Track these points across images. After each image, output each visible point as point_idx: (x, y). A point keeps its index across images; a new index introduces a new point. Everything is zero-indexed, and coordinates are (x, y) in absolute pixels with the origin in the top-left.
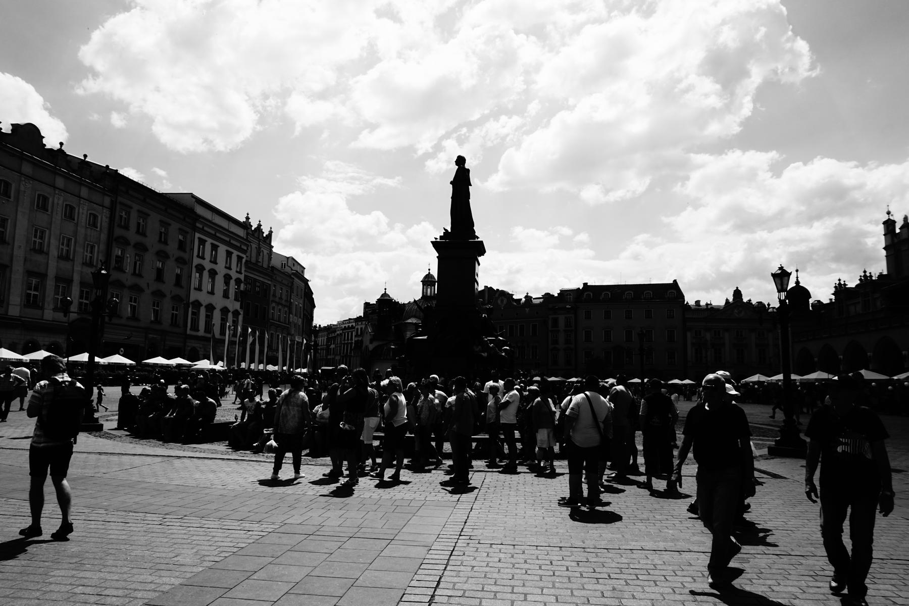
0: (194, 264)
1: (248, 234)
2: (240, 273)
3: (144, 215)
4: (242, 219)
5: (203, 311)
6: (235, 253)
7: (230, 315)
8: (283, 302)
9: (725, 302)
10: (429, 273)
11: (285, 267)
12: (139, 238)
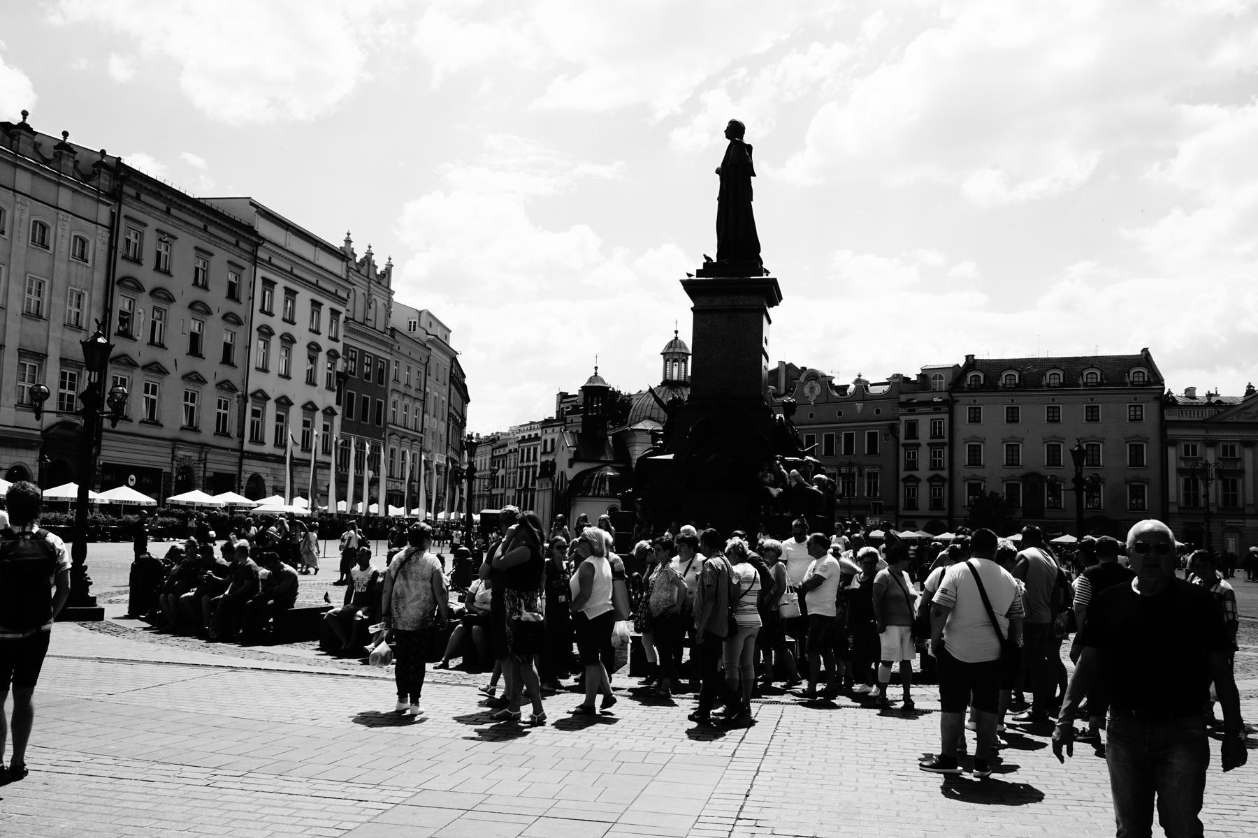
0: (255, 326)
1: (348, 269)
2: (336, 340)
3: (166, 238)
4: (338, 243)
5: (271, 410)
6: (327, 304)
7: (319, 416)
8: (412, 392)
9: (1245, 391)
10: (676, 338)
11: (414, 330)
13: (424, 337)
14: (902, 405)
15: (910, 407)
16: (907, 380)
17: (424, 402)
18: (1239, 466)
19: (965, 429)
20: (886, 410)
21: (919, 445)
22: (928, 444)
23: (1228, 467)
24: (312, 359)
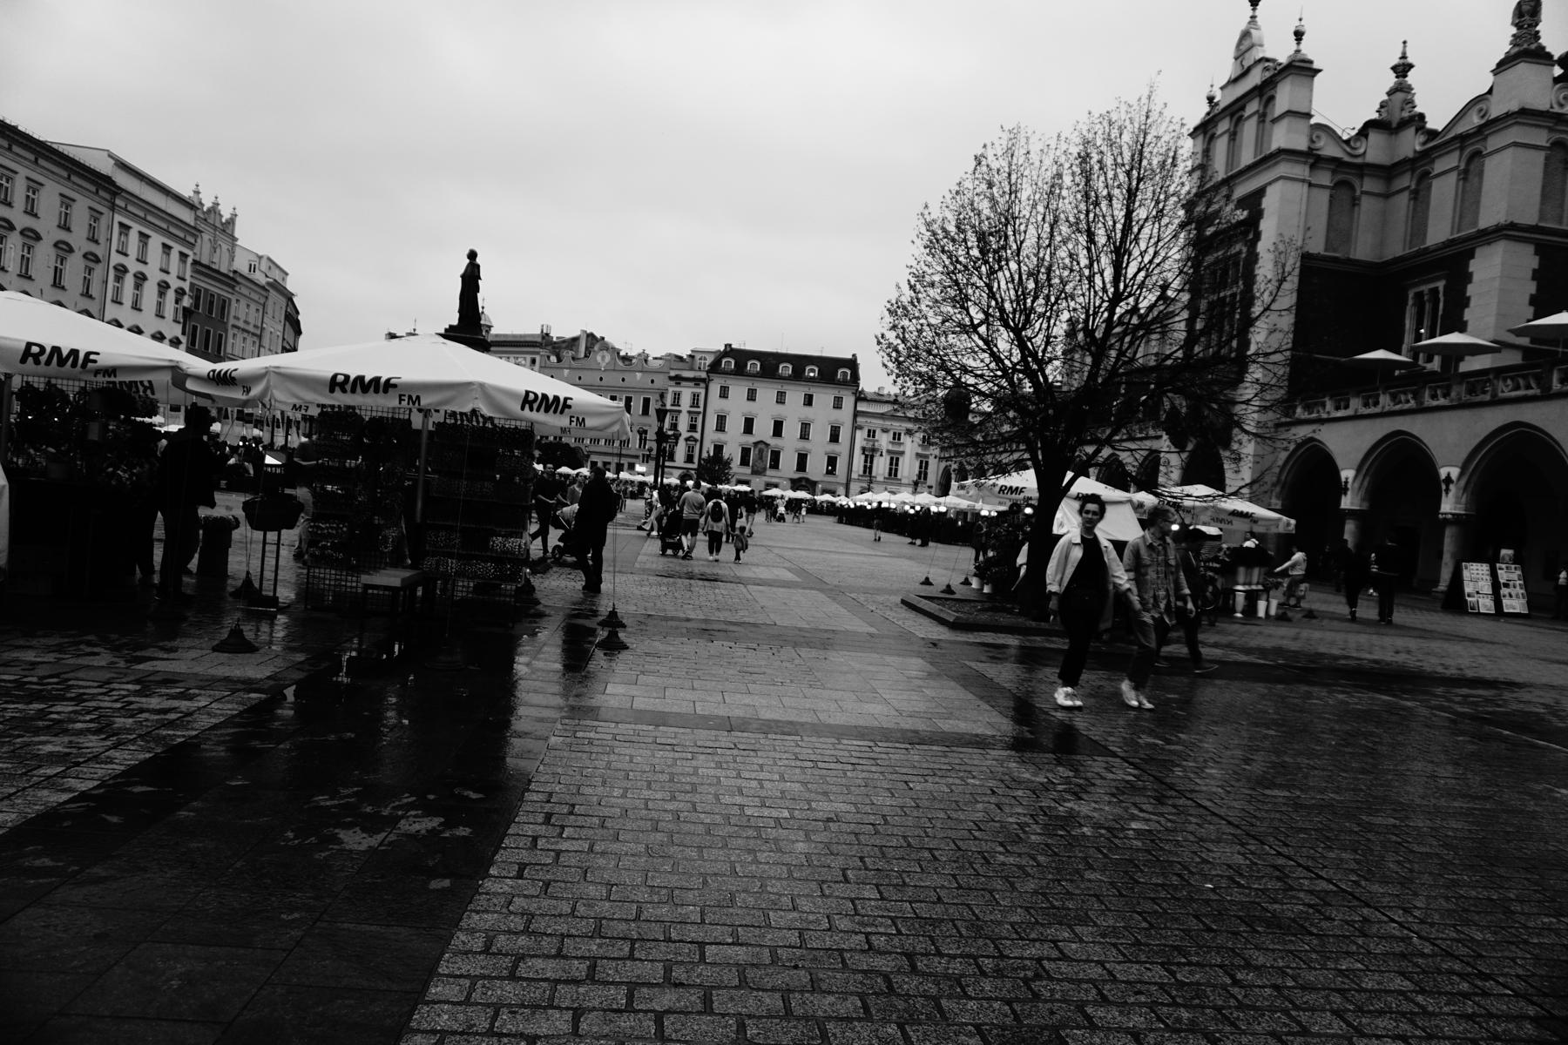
0: (112, 264)
1: (197, 218)
2: (183, 279)
3: (34, 186)
4: (186, 192)
6: (177, 248)
8: (251, 328)
12: (28, 222)
13: (262, 280)
14: (671, 378)
15: (678, 380)
16: (680, 358)
17: (260, 337)
18: (901, 449)
19: (716, 404)
20: (661, 381)
21: (680, 412)
22: (689, 412)
23: (896, 448)
24: (162, 294)
